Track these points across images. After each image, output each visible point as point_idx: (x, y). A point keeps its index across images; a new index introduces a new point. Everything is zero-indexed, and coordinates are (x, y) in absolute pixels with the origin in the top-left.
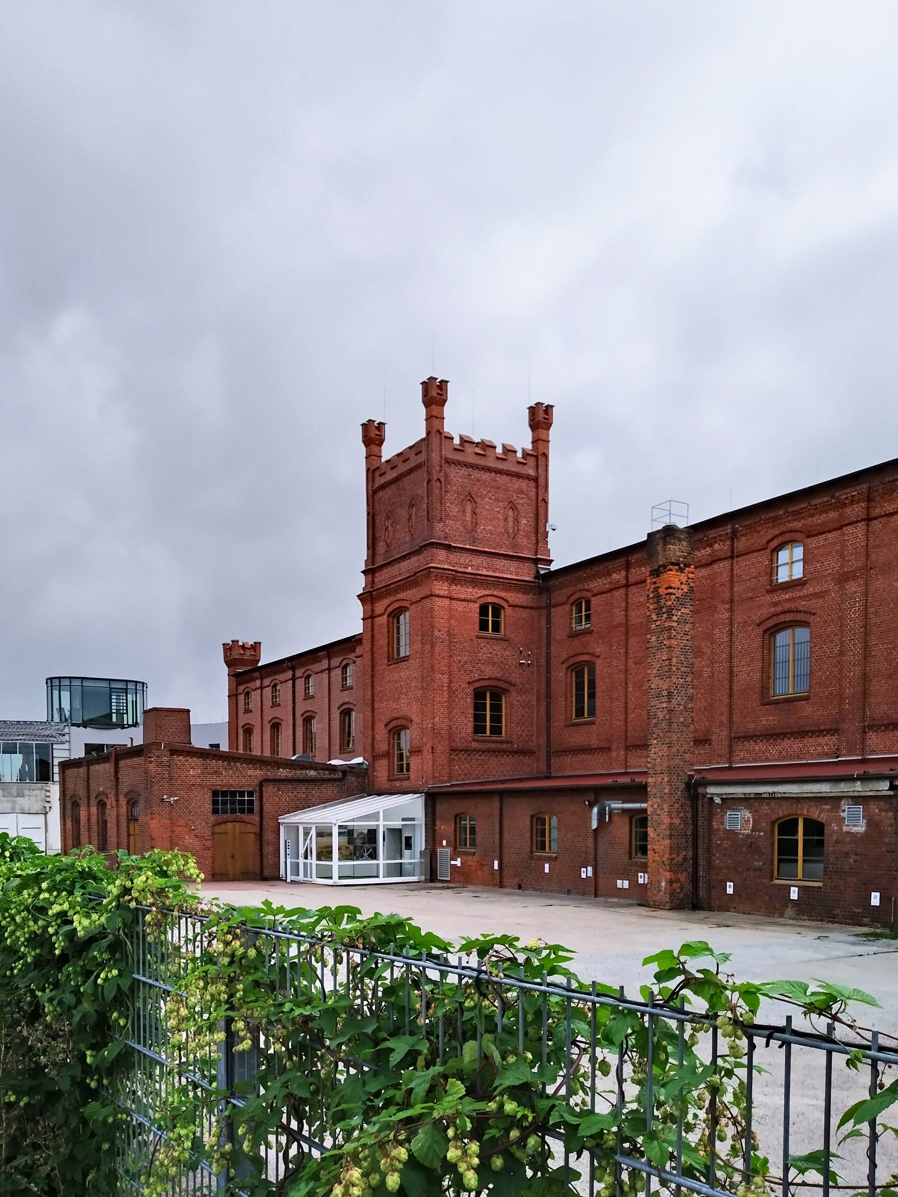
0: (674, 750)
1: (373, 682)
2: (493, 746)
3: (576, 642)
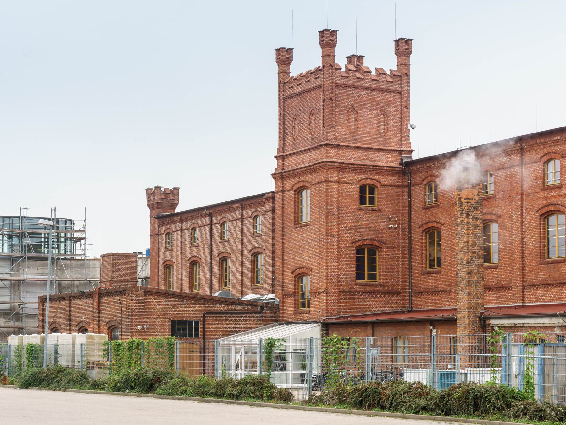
0: (471, 297)
1: (283, 239)
2: (370, 288)
3: (428, 213)
